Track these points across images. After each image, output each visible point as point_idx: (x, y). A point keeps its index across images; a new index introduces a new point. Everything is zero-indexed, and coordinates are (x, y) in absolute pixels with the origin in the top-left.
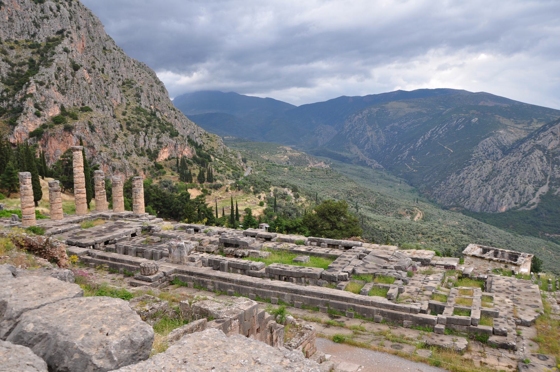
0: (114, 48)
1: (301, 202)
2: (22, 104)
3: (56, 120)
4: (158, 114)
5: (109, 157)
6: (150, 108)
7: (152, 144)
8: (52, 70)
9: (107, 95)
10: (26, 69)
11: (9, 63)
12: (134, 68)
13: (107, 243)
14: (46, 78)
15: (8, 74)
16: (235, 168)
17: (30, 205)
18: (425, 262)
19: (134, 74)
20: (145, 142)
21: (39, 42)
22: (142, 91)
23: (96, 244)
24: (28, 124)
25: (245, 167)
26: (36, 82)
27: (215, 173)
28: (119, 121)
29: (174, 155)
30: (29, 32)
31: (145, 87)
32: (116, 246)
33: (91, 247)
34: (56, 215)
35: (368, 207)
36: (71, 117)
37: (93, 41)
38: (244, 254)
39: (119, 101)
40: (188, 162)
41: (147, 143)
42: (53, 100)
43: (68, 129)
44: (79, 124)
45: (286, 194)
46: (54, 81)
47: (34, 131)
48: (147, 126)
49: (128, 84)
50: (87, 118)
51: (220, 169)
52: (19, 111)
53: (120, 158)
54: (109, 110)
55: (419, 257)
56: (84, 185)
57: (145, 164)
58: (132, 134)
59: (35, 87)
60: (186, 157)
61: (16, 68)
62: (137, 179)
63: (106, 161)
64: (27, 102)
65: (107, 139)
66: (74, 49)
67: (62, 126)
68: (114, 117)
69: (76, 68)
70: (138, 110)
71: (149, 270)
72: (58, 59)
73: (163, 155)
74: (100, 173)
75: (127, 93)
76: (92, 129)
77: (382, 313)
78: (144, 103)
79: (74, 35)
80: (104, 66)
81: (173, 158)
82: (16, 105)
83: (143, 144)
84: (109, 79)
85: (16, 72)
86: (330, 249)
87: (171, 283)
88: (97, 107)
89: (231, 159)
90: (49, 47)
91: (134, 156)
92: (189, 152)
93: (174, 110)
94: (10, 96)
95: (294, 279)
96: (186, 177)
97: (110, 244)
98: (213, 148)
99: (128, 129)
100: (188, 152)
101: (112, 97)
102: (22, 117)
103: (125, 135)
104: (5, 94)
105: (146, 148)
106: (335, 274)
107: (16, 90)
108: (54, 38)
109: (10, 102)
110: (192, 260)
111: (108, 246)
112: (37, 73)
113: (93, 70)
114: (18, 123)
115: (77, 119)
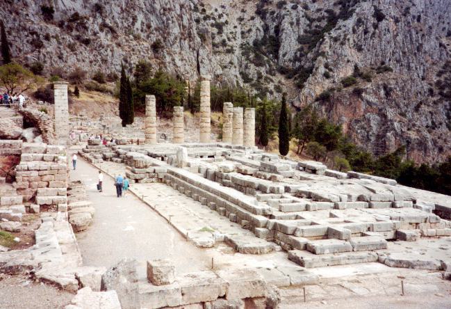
2: (314, 65)
3: (346, 82)
5: (405, 129)
8: (350, 23)
10: (324, 23)
14: (342, 34)
15: (305, 31)
17: (151, 125)
23: (165, 156)
24: (316, 87)
28: (431, 84)
33: (160, 158)
36: (364, 78)
39: (436, 57)
42: (346, 60)
43: (358, 93)
46: (351, 37)
47: (321, 95)
52: (310, 71)
59: (329, 43)
64: (317, 61)
65: (407, 106)
67: (351, 89)
76: (387, 94)
77: (238, 213)
82: (307, 65)
85: (314, 28)
94: (301, 55)
101: (425, 52)
102: (311, 78)
107: (310, 49)
109: (303, 63)
112: (334, 27)
113: (403, 19)
115: (369, 81)
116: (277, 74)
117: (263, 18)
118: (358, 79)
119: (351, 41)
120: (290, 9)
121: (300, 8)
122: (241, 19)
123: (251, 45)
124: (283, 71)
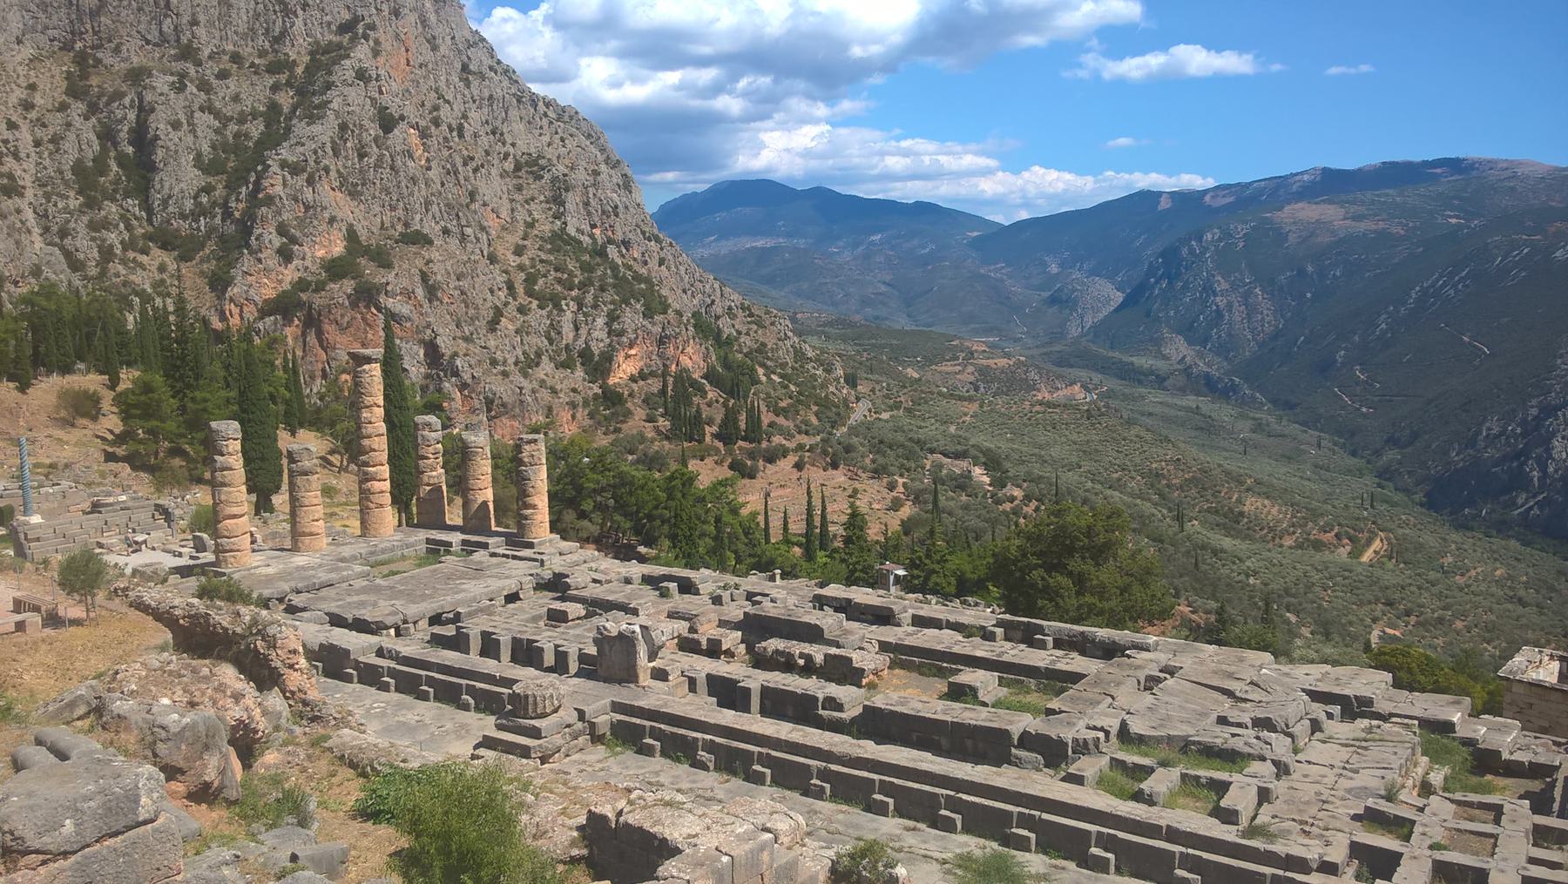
0: (491, 68)
1: (1012, 499)
3: (335, 269)
4: (612, 251)
6: (592, 236)
7: (595, 334)
8: (325, 130)
9: (473, 200)
10: (256, 129)
11: (217, 115)
12: (545, 122)
13: (435, 620)
15: (213, 147)
16: (824, 404)
17: (235, 510)
18: (1354, 708)
19: (546, 139)
20: (577, 329)
21: (293, 56)
22: (567, 190)
25: (853, 399)
26: (284, 164)
27: (766, 418)
28: (506, 272)
29: (657, 363)
30: (267, 30)
31: (581, 176)
32: (458, 628)
33: (392, 631)
34: (307, 540)
35: (1212, 518)
37: (435, 48)
38: (809, 658)
39: (504, 214)
40: (694, 384)
41: (583, 332)
42: (326, 215)
43: (367, 295)
44: (399, 279)
45: (967, 475)
48: (583, 286)
49: (531, 166)
50: (419, 263)
51: (783, 404)
53: (505, 374)
54: (478, 240)
55: (1337, 690)
56: (385, 456)
57: (574, 390)
58: (541, 307)
60: (686, 370)
61: (233, 127)
62: (529, 442)
63: (469, 381)
66: (382, 72)
67: (348, 286)
68: (493, 259)
69: (387, 122)
70: (560, 240)
71: (535, 703)
72: (339, 100)
73: (624, 369)
74: (429, 425)
75: (527, 193)
78: (575, 224)
79: (384, 35)
80: (465, 117)
81: (652, 374)
83: (571, 335)
84: (479, 155)
86: (1059, 653)
87: (597, 739)
88: (446, 231)
89: (814, 377)
90: (318, 69)
91: (546, 366)
92: (698, 358)
93: (658, 240)
94: (214, 204)
95: (944, 742)
96: (687, 428)
97: (449, 621)
98: (764, 345)
99: (530, 293)
100: (693, 358)
101: (485, 205)
102: (247, 262)
103: (522, 310)
104: (204, 199)
105: (581, 343)
106: (1068, 735)
108: (330, 42)
110: (660, 675)
111: (437, 630)
112: (286, 137)
114: (233, 278)
115: (388, 265)
116: (156, 251)
117: (93, 109)
118: (363, 261)
119: (333, 174)
120: (166, 89)
121: (191, 88)
122: (27, 106)
123: (69, 175)
124: (165, 240)
